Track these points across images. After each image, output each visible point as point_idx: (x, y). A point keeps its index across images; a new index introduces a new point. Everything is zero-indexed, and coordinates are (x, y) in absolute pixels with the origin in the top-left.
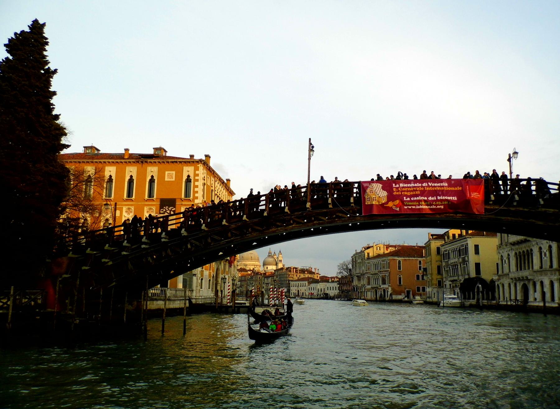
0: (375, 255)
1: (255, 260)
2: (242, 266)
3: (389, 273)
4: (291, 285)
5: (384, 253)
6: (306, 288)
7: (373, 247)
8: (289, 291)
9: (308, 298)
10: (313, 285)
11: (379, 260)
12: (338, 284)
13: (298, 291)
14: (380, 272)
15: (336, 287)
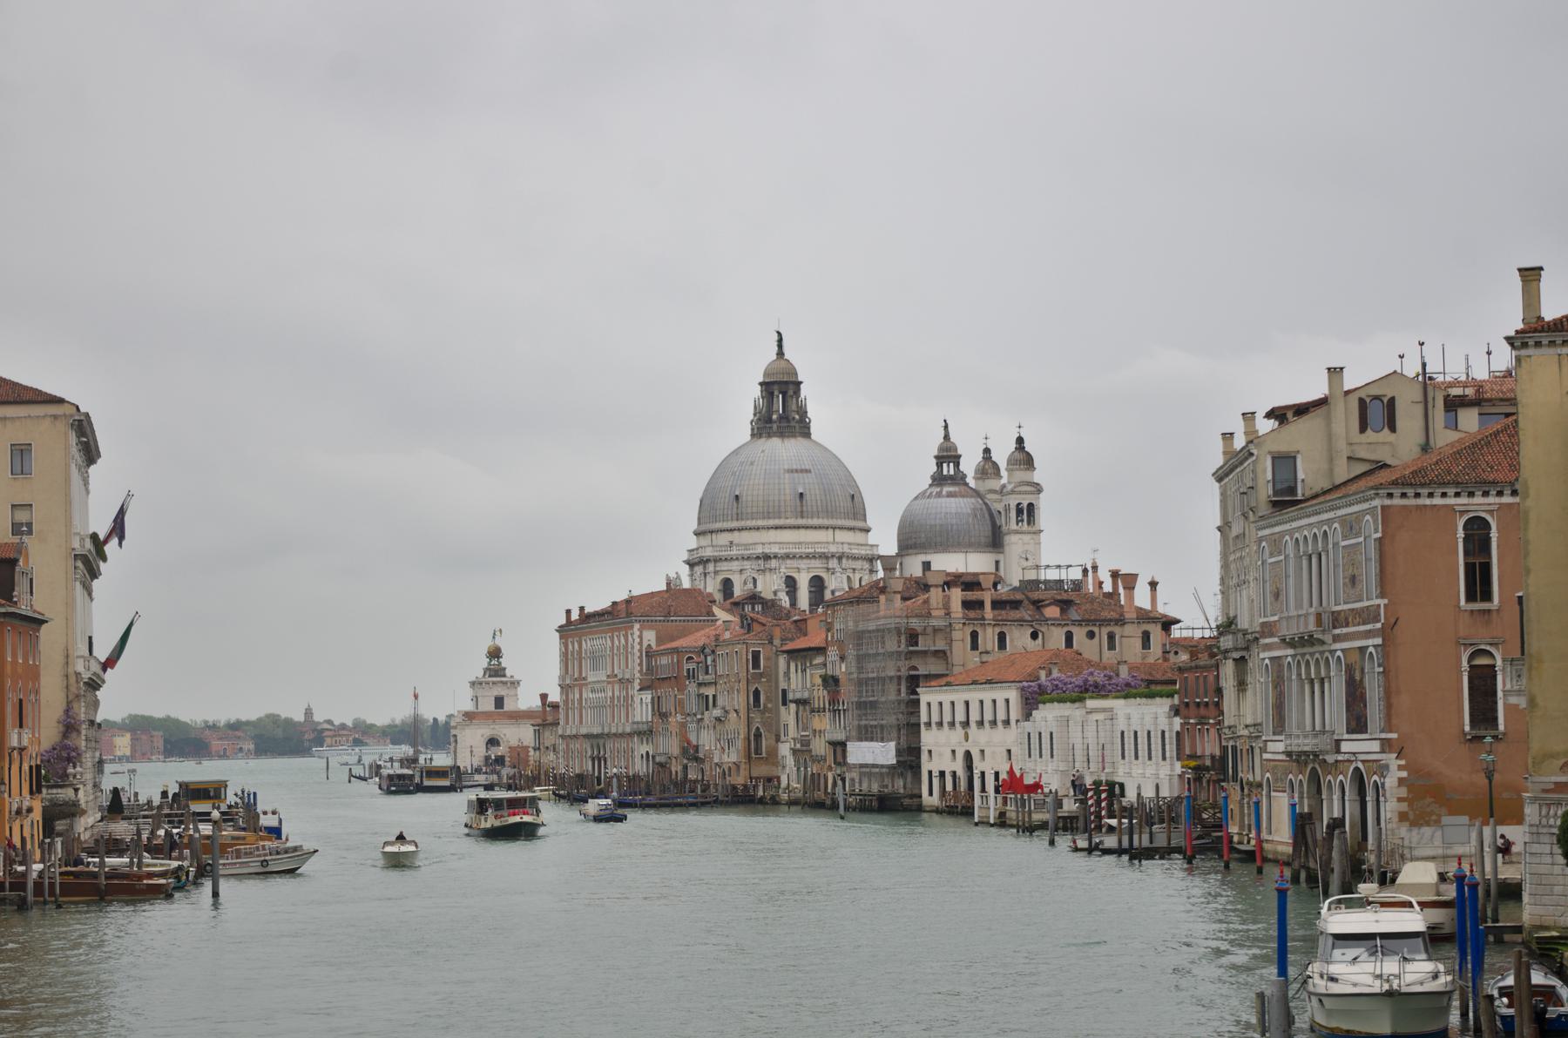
0: (1342, 472)
1: (830, 513)
2: (735, 565)
3: (1383, 632)
4: (924, 718)
5: (1425, 448)
6: (1009, 737)
7: (1322, 403)
8: (910, 758)
9: (984, 823)
10: (1048, 715)
11: (1329, 522)
12: (1176, 711)
13: (968, 755)
14: (1338, 620)
15: (1163, 732)
